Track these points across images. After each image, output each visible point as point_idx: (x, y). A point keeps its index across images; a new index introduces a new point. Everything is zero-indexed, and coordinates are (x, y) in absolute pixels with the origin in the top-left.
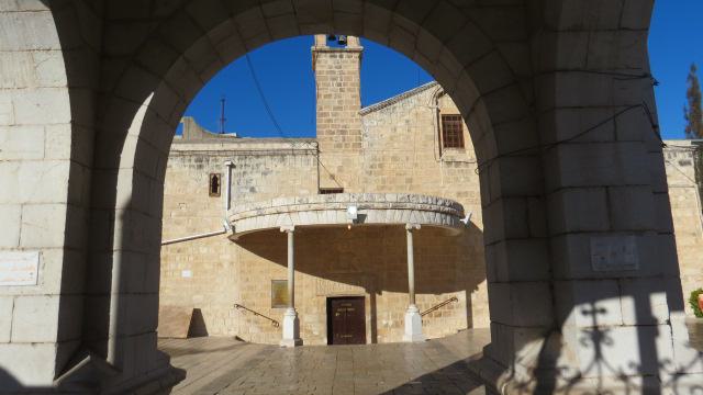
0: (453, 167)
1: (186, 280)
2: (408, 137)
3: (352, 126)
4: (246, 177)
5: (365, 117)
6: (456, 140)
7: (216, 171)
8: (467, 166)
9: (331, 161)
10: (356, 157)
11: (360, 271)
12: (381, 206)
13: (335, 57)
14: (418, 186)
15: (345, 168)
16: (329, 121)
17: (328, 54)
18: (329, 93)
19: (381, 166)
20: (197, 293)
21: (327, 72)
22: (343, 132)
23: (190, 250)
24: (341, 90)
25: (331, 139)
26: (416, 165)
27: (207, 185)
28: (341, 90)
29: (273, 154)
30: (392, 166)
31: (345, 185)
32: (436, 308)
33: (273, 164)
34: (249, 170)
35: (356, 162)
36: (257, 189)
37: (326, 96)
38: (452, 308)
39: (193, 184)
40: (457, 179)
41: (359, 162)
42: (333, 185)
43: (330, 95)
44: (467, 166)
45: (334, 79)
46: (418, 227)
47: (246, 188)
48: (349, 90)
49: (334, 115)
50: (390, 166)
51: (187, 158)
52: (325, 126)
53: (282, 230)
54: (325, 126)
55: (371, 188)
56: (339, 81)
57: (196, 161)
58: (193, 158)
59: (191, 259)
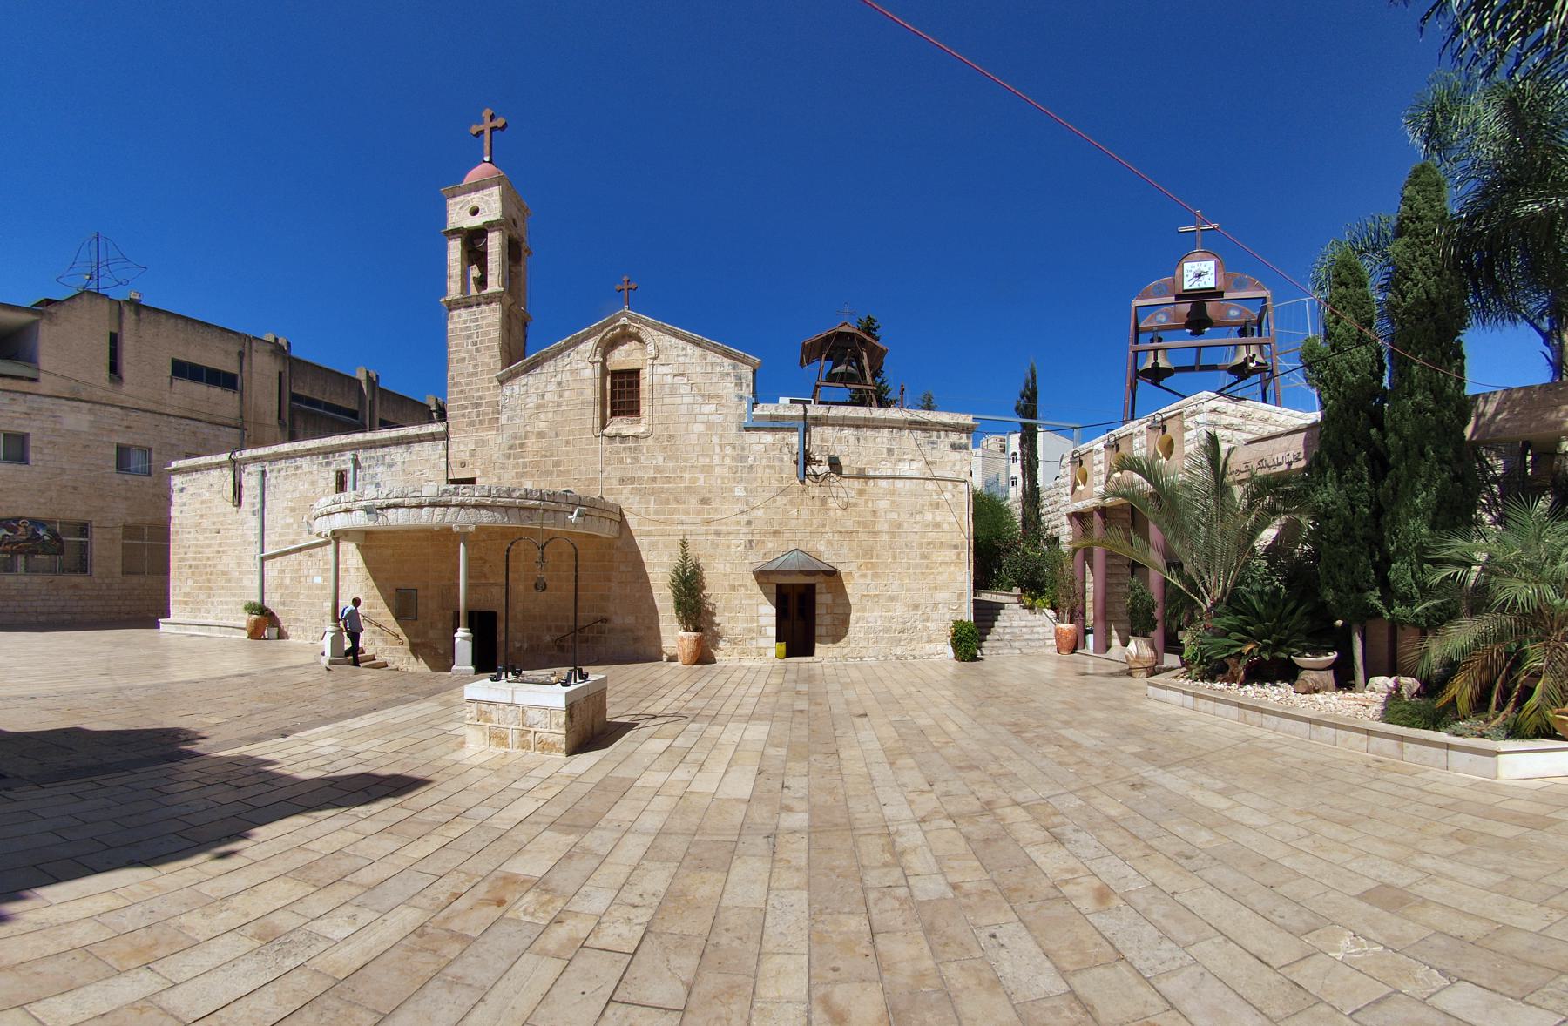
0: (617, 444)
2: (559, 405)
3: (489, 396)
8: (637, 441)
9: (462, 444)
10: (491, 436)
15: (479, 453)
19: (522, 446)
26: (567, 443)
31: (477, 473)
33: (397, 453)
35: (491, 443)
39: (322, 483)
40: (621, 461)
41: (497, 441)
44: (637, 441)
50: (533, 445)
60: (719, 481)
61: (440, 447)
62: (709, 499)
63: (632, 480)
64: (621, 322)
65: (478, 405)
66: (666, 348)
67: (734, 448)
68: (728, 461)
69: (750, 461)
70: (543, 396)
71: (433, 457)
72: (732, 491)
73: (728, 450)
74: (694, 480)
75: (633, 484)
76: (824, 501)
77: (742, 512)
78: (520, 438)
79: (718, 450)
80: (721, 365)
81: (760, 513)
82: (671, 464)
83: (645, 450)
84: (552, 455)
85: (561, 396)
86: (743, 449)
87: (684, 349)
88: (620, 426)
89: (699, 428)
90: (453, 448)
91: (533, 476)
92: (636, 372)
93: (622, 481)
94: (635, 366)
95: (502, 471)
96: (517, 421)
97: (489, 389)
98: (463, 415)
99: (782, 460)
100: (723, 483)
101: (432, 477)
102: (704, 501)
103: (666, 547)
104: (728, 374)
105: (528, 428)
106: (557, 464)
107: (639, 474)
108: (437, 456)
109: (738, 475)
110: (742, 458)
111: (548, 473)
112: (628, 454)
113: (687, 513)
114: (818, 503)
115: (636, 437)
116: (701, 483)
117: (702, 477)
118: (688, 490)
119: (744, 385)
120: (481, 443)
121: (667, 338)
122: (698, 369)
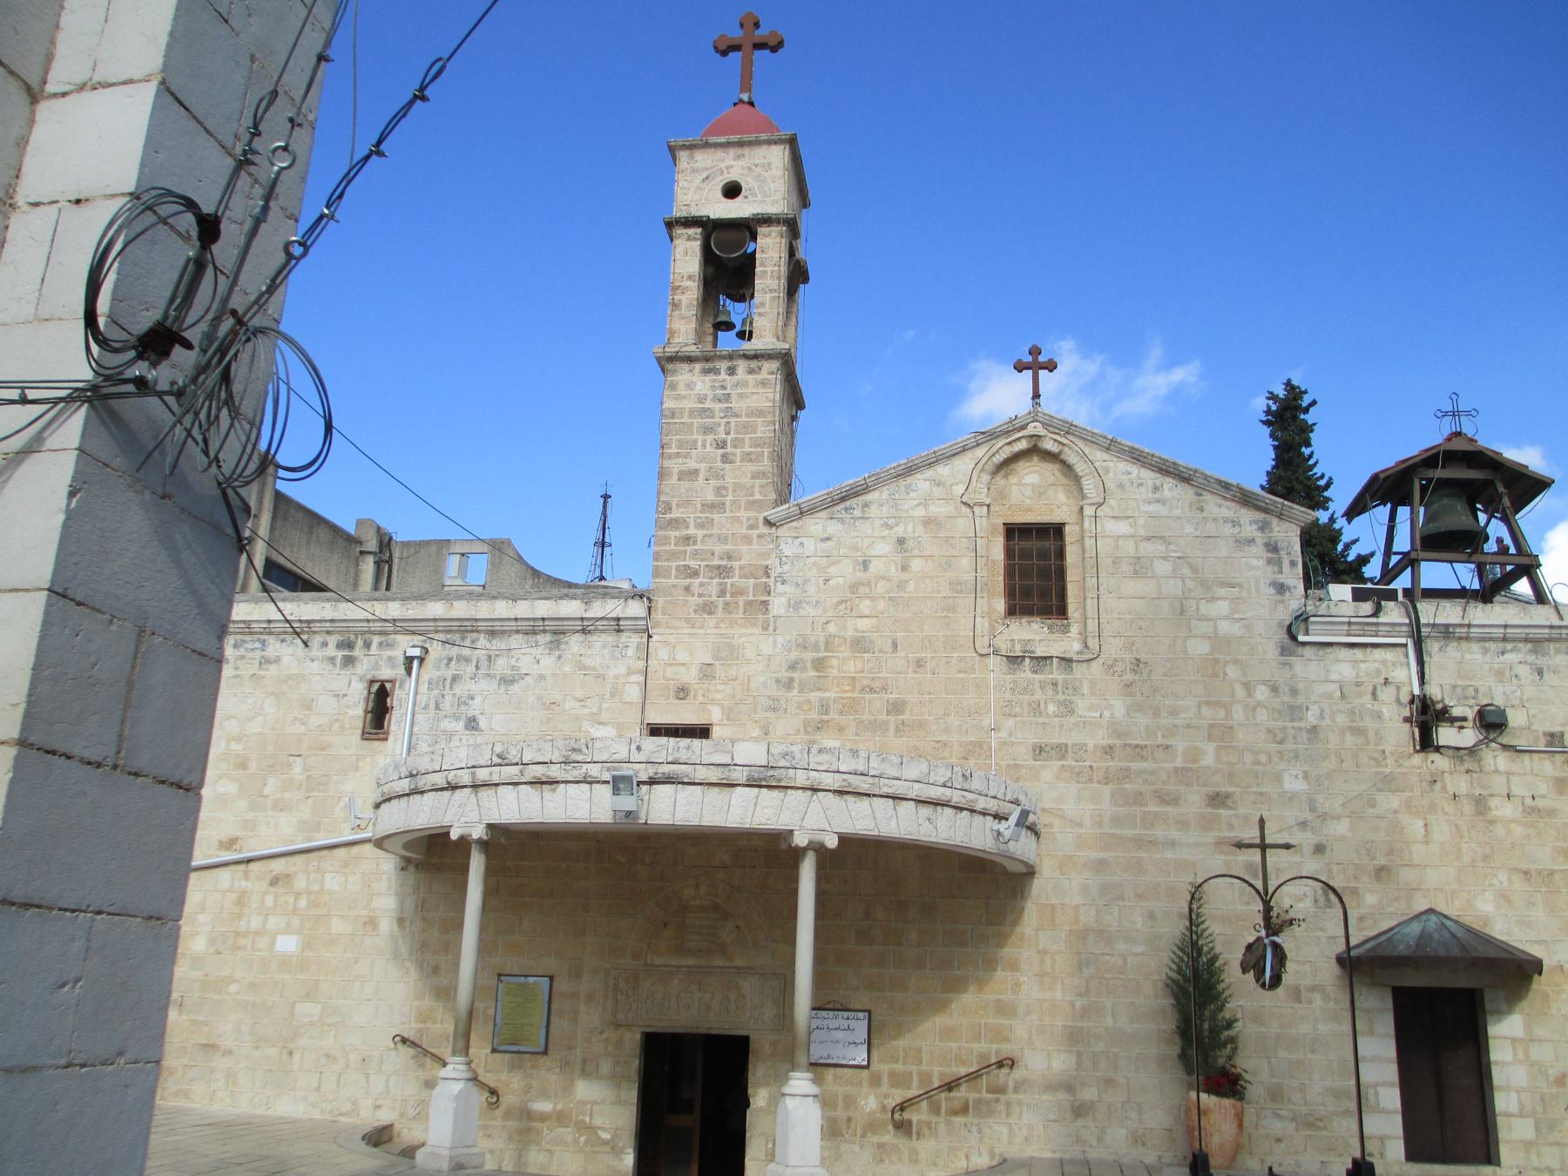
0: (1026, 673)
1: (285, 963)
2: (901, 585)
3: (748, 555)
4: (459, 689)
5: (783, 531)
6: (1044, 594)
7: (385, 673)
11: (739, 962)
12: (714, 775)
13: (716, 372)
14: (921, 724)
15: (720, 672)
16: (688, 539)
17: (698, 367)
18: (692, 465)
19: (819, 664)
20: (310, 995)
21: (692, 413)
22: (722, 571)
23: (300, 883)
24: (726, 459)
25: (687, 589)
26: (920, 664)
27: (357, 709)
28: (726, 459)
29: (533, 628)
30: (851, 667)
31: (714, 716)
32: (950, 1086)
33: (529, 657)
34: (471, 669)
35: (749, 653)
36: (483, 723)
37: (682, 476)
38: (1000, 1090)
39: (327, 705)
40: (1036, 708)
42: (686, 715)
43: (696, 472)
45: (707, 430)
46: (832, 842)
47: (456, 718)
48: (748, 457)
49: (701, 526)
50: (845, 664)
51: (316, 640)
52: (672, 556)
53: (454, 836)
54: (672, 556)
55: (786, 726)
56: (710, 438)
57: (340, 646)
58: (333, 640)
59: (303, 903)
60: (1248, 758)
61: (631, 652)
62: (1228, 796)
63: (1061, 750)
64: (1030, 430)
65: (722, 571)
66: (1121, 486)
67: (1275, 689)
68: (1262, 715)
69: (1311, 718)
70: (865, 565)
71: (612, 673)
72: (1278, 778)
73: (1262, 693)
74: (1194, 755)
75: (1063, 757)
76: (1480, 804)
77: (1303, 825)
78: (816, 647)
79: (1240, 692)
80: (1235, 523)
81: (1341, 828)
82: (1143, 720)
83: (1085, 690)
84: (884, 689)
85: (904, 568)
86: (1294, 692)
87: (1156, 489)
88: (1032, 633)
89: (1200, 648)
90: (660, 654)
91: (841, 729)
92: (1057, 530)
93: (1039, 751)
94: (1056, 518)
95: (770, 715)
96: (809, 610)
97: (747, 540)
98: (687, 589)
99: (1378, 716)
100: (1258, 763)
101: (605, 716)
102: (1218, 800)
103: (1140, 896)
104: (1251, 541)
105: (832, 628)
106: (896, 708)
107: (1071, 738)
108: (623, 670)
109: (1289, 746)
110: (1295, 711)
111: (875, 726)
112: (1050, 692)
113: (1183, 825)
114: (1468, 808)
115: (1066, 661)
116: (1209, 760)
117: (1210, 748)
118: (1183, 774)
119: (1286, 565)
120: (728, 652)
121: (1123, 466)
122: (1189, 529)
